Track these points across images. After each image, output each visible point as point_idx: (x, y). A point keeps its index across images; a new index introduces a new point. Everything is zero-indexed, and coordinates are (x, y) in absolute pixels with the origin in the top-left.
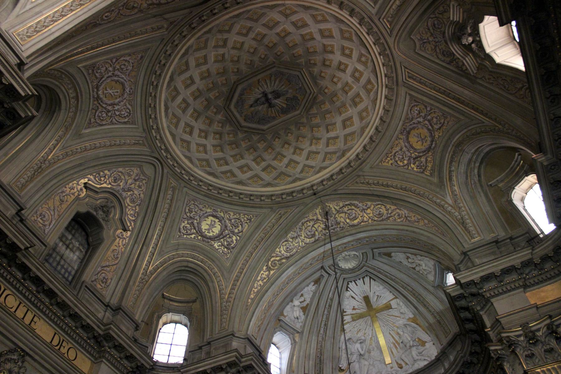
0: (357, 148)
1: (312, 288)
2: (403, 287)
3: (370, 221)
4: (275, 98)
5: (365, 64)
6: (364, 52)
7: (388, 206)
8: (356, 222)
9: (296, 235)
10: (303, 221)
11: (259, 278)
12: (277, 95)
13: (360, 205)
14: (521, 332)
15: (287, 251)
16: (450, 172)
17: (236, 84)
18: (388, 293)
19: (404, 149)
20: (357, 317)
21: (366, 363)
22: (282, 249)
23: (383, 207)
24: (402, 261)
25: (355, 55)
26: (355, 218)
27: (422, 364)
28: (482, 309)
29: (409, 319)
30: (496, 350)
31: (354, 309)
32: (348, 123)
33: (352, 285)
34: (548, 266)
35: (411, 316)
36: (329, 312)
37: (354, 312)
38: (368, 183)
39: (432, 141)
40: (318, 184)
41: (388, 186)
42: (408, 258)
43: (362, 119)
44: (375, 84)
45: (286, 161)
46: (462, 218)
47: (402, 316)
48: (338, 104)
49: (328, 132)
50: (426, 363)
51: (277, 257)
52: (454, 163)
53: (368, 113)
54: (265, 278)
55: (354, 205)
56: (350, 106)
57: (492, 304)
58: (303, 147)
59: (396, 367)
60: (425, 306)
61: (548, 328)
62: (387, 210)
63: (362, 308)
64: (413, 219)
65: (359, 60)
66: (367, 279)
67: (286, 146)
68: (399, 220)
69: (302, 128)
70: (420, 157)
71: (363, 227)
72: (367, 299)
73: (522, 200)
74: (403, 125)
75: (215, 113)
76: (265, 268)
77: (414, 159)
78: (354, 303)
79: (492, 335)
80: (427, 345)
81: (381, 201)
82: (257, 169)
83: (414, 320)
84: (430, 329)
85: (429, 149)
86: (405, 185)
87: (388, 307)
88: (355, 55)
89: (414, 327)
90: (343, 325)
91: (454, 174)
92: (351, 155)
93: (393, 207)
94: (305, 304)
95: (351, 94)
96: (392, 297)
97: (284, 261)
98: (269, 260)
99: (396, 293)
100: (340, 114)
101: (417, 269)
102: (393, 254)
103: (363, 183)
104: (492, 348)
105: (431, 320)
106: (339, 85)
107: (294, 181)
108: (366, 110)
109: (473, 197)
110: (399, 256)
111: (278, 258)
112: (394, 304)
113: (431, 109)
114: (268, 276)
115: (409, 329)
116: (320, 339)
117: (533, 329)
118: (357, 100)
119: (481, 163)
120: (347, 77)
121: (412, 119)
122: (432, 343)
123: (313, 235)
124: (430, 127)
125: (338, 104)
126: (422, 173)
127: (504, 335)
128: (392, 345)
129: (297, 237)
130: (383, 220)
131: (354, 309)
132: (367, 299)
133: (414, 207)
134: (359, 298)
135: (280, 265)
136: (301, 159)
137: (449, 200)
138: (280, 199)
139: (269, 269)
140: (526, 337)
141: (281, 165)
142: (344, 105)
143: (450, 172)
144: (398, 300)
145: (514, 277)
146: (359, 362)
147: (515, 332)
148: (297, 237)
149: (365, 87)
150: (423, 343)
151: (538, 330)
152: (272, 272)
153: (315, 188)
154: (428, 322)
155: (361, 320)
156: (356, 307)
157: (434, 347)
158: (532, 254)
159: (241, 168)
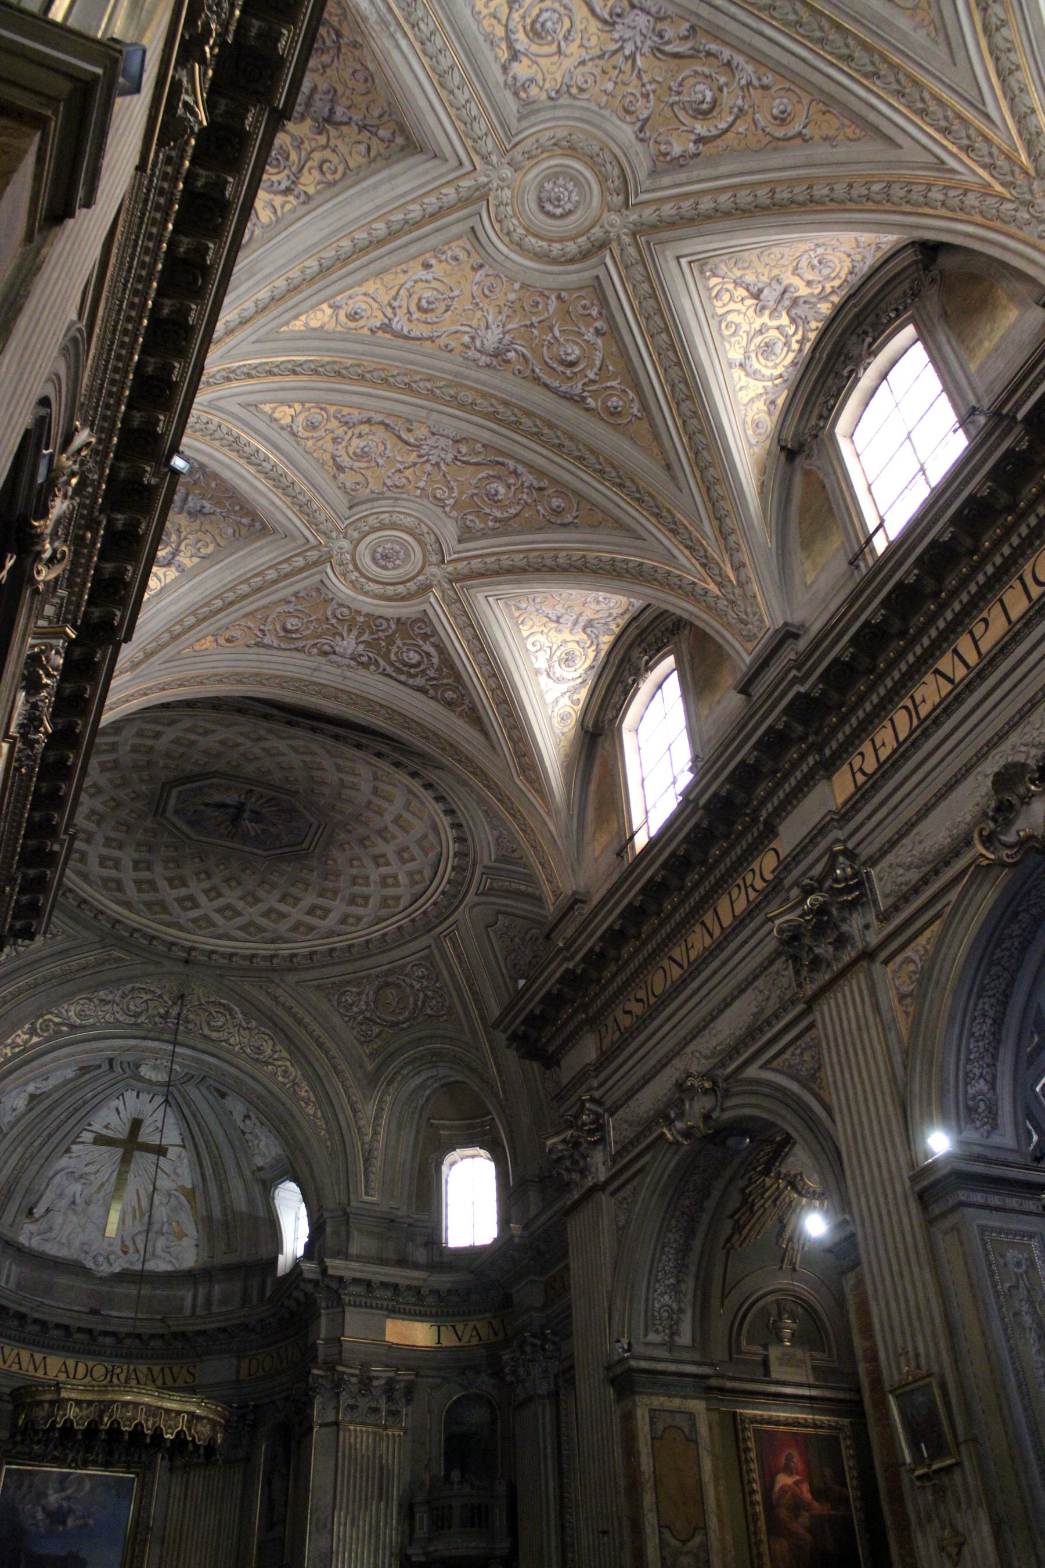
0: (302, 947)
1: (70, 1074)
2: (206, 1142)
3: (237, 1048)
4: (251, 821)
5: (414, 883)
6: (427, 873)
7: (278, 1048)
8: (214, 1035)
9: (110, 997)
10: (138, 985)
11: (9, 1041)
12: (257, 816)
13: (240, 1016)
14: (357, 1372)
15: (78, 1015)
16: (398, 1072)
17: (213, 774)
18: (176, 1133)
19: (364, 997)
20: (101, 1140)
21: (74, 1219)
22: (72, 1008)
23: (271, 1043)
24: (235, 1113)
25: (411, 866)
26: (218, 1030)
27: (162, 1266)
28: (327, 1308)
29: (182, 1189)
30: (319, 1376)
31: (106, 1127)
32: (319, 912)
33: (130, 1096)
34: (430, 1300)
35: (189, 1186)
36: (68, 1118)
37: (104, 1132)
38: (275, 999)
39: (407, 1020)
40: (203, 950)
41: (299, 1022)
42: (247, 1117)
43: (343, 921)
44: (401, 907)
45: (183, 892)
46: (370, 1151)
47: (173, 1176)
48: (329, 885)
49: (282, 899)
50: (170, 1268)
51: (57, 1016)
52: (410, 1067)
53: (357, 924)
54: (19, 1046)
55: (230, 1011)
56: (342, 899)
57: (343, 1312)
58: (225, 890)
59: (117, 1248)
60: (220, 1188)
61: (387, 1383)
62: (274, 1051)
63: (119, 1129)
64: (303, 1094)
65: (411, 874)
66: (159, 1100)
67: (203, 876)
68: (280, 1079)
69: (248, 872)
70: (376, 1023)
71: (222, 1048)
72: (136, 1124)
73: (452, 1164)
74: (389, 970)
75: (142, 780)
76: (27, 1026)
77: (366, 1018)
78: (113, 1120)
79: (321, 1352)
80: (186, 1242)
81: (275, 1033)
82: (128, 875)
83: (190, 1194)
84: (207, 1223)
85: (394, 1025)
86: (325, 1038)
87: (160, 1151)
88: (411, 866)
89: (181, 1204)
90: (74, 1142)
91: (399, 1078)
92: (285, 949)
93: (284, 1054)
94: (39, 1092)
95: (357, 889)
96: (179, 1141)
97: (65, 1029)
98: (42, 1016)
99: (189, 1143)
100: (321, 896)
101: (249, 1137)
102: (229, 1099)
103: (268, 994)
104: (315, 1371)
105: (217, 1213)
106: (354, 871)
107: (170, 925)
108: (359, 919)
109: (400, 1126)
110: (237, 1107)
111: (57, 1020)
112: (172, 1153)
113: (440, 988)
114: (26, 1042)
115: (173, 1202)
116: (27, 1155)
117: (373, 1374)
118: (360, 901)
119: (442, 1086)
120: (374, 874)
121: (406, 975)
122: (195, 1242)
123: (137, 1015)
124: (420, 1003)
125: (329, 885)
126: (361, 1043)
127: (340, 1368)
128: (130, 1210)
129: (109, 1002)
130: (257, 1060)
131: (106, 1127)
132: (136, 1124)
133: (316, 1081)
134: (127, 1116)
135: (56, 1032)
136: (207, 906)
137: (370, 1110)
138: (126, 934)
139: (33, 1032)
140: (360, 1382)
141: (170, 894)
142: (335, 893)
143: (398, 1072)
144: (184, 1153)
145: (389, 1294)
146: (65, 1214)
147: (351, 1372)
148: (109, 1002)
149: (385, 899)
150: (181, 1235)
151: (377, 1378)
152: (35, 1039)
153: (194, 953)
154: (209, 1210)
155: (105, 1148)
156: (112, 1126)
157: (194, 1250)
158: (425, 1280)
159: (103, 861)
